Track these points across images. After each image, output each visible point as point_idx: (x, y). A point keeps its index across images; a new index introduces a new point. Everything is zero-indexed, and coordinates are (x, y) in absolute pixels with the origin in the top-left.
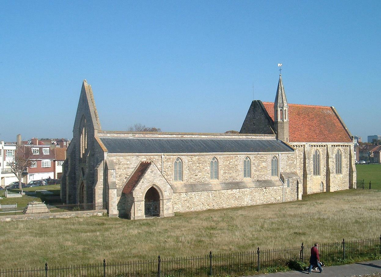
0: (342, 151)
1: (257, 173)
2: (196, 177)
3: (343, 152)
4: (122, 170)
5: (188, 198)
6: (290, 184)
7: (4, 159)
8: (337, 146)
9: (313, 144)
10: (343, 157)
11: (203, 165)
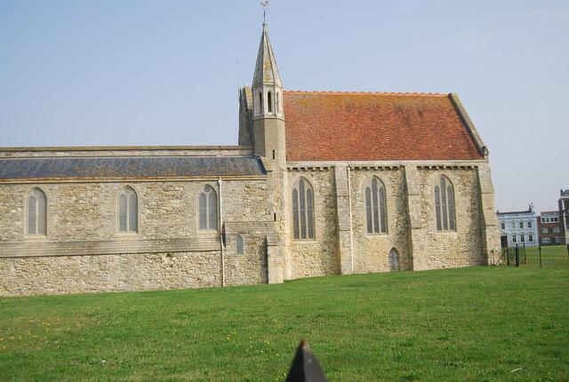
1: (155, 223)
6: (245, 247)
8: (434, 167)
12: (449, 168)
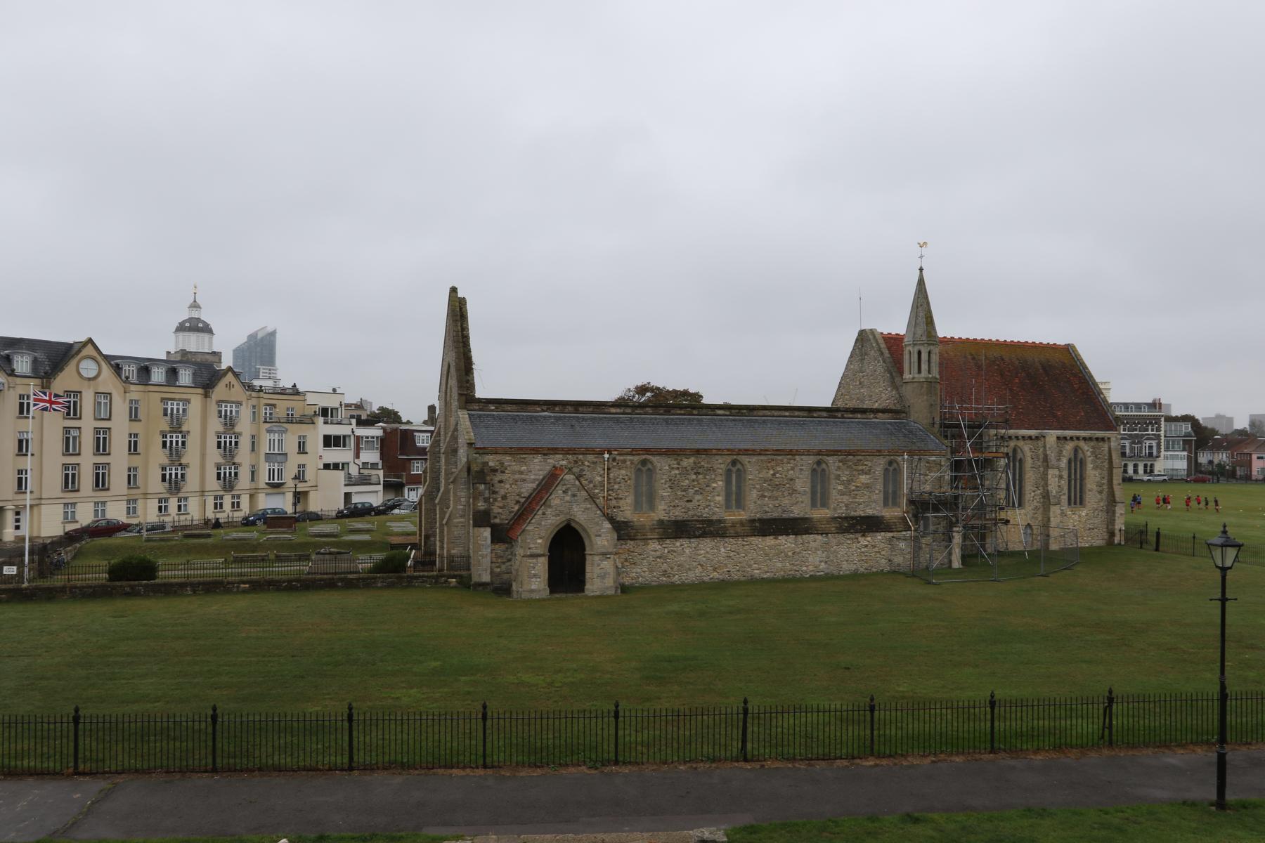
0: (1088, 451)
1: (846, 499)
2: (689, 505)
4: (507, 486)
5: (666, 551)
7: (357, 456)
8: (1071, 438)
9: (1068, 433)
10: (1090, 466)
11: (707, 477)
12: (1085, 439)
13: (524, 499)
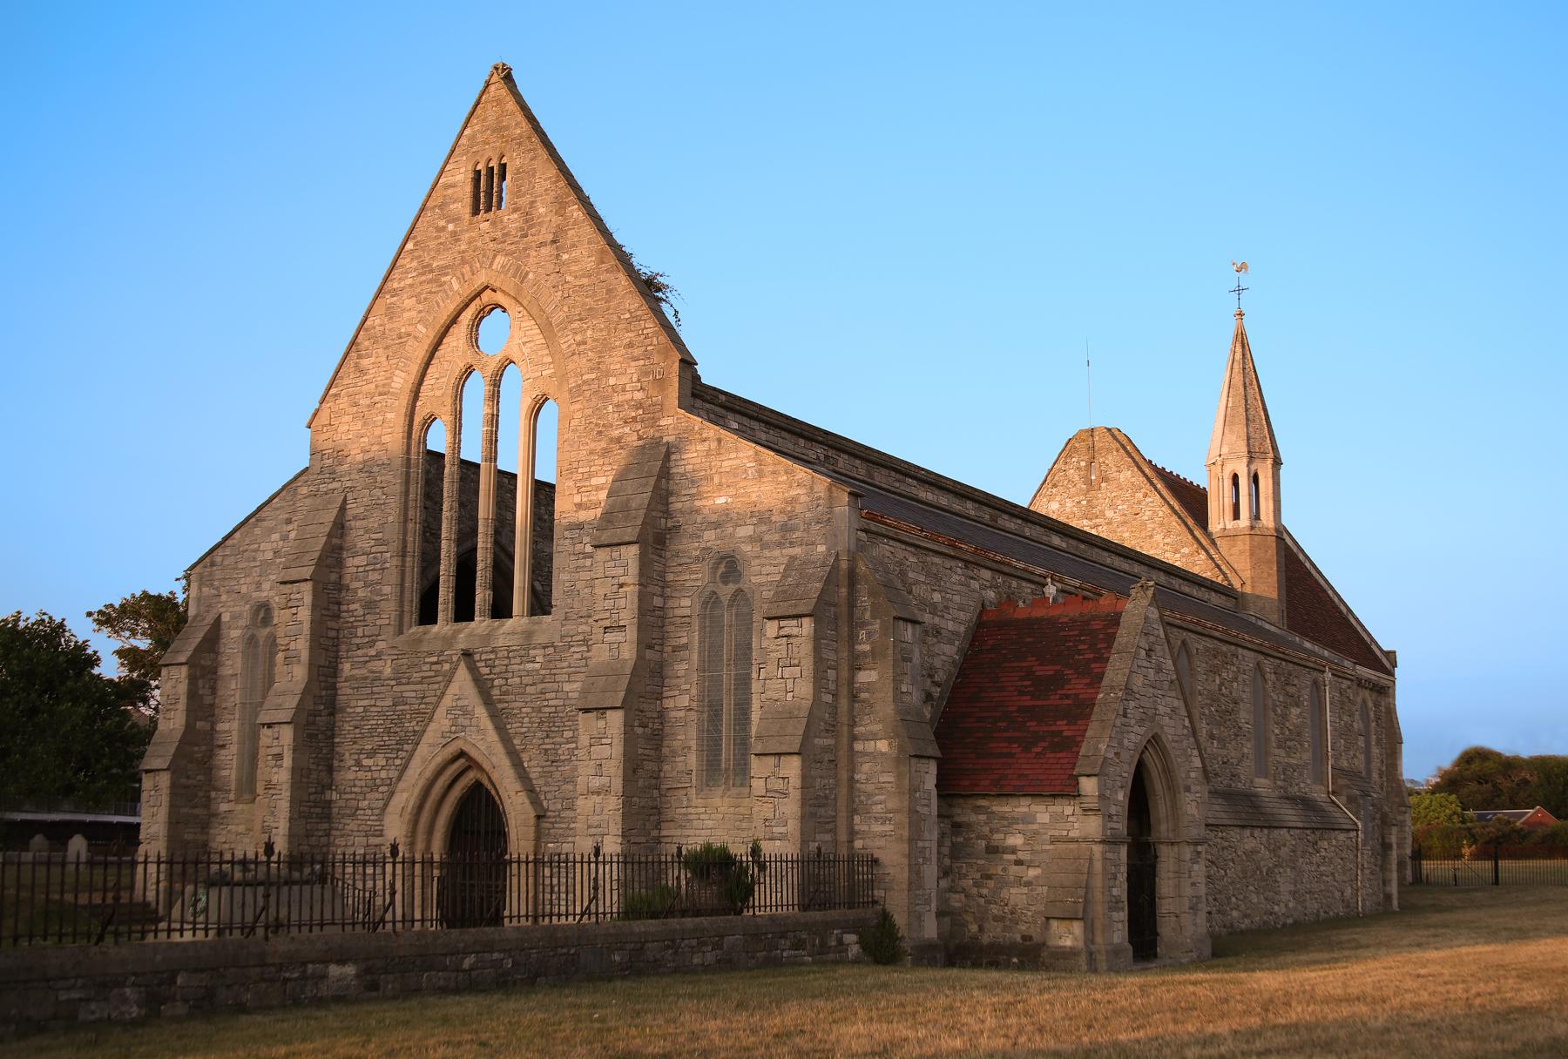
3: (1372, 715)
13: (939, 690)
